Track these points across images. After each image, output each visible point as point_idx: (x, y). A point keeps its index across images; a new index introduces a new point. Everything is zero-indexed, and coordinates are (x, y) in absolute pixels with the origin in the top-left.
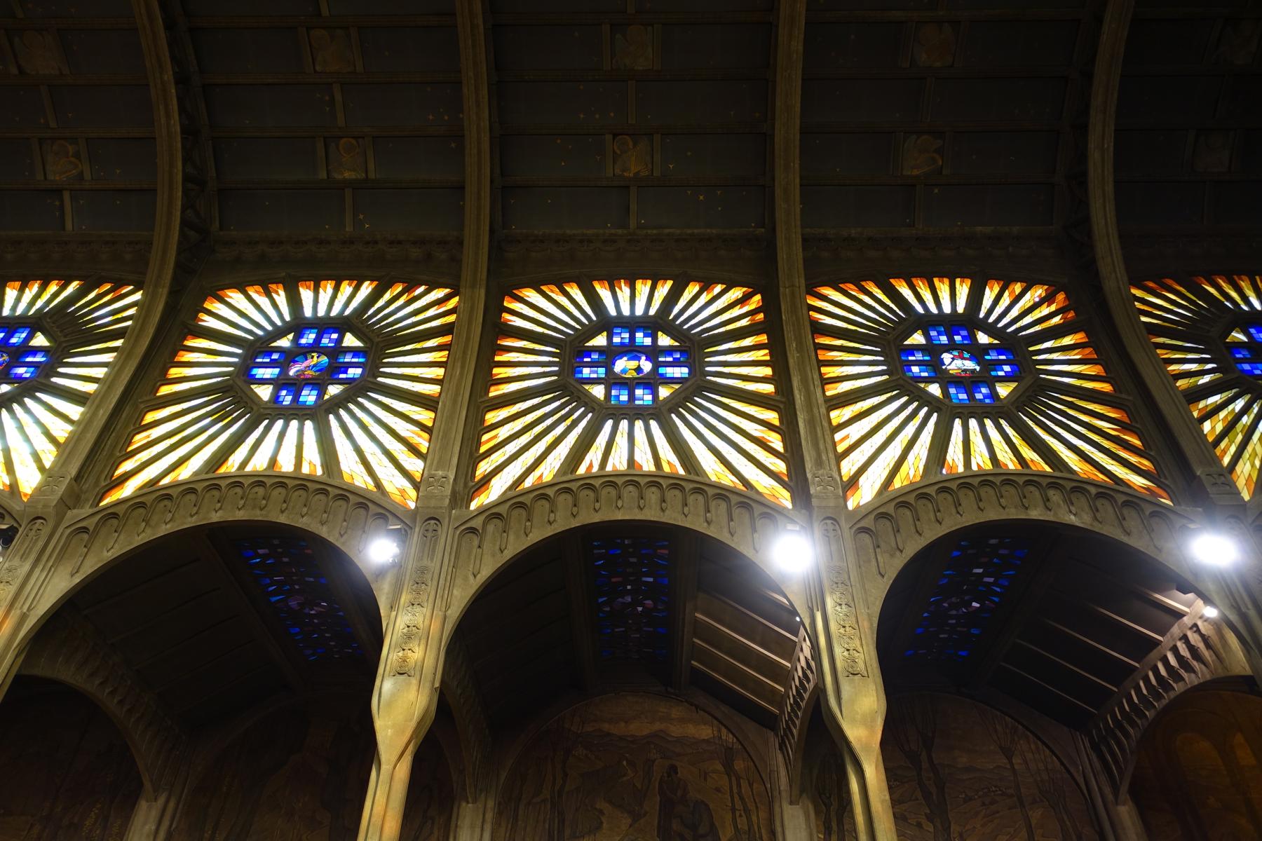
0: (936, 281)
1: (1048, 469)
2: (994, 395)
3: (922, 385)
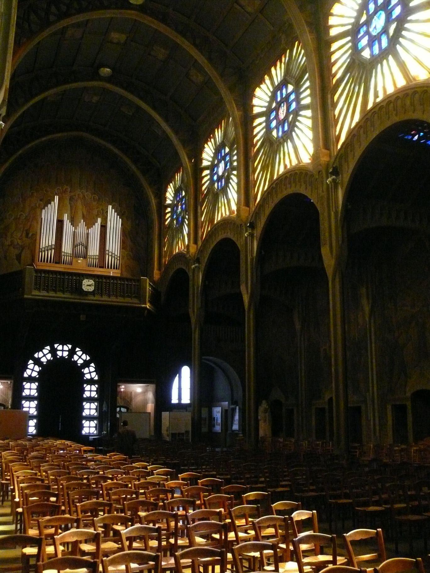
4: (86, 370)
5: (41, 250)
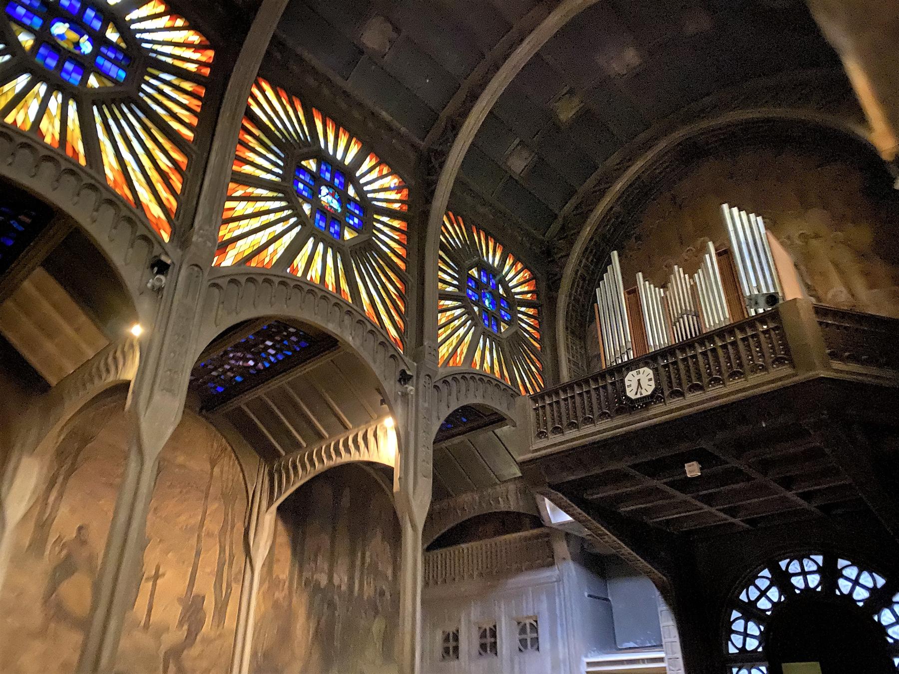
0: (341, 130)
1: (350, 301)
2: (340, 234)
3: (301, 200)
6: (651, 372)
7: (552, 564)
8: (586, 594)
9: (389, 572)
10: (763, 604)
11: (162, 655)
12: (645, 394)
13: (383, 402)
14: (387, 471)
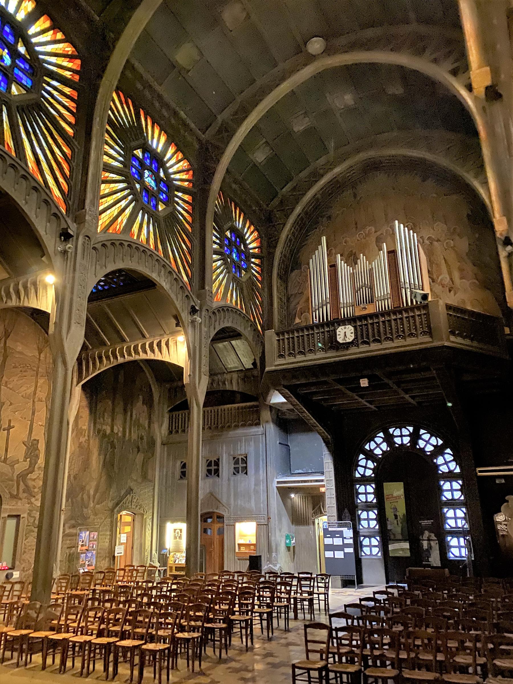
2: (156, 207)
4: (440, 460)
5: (314, 310)
6: (353, 328)
7: (258, 424)
8: (278, 442)
9: (146, 425)
10: (378, 452)
11: (15, 478)
12: (348, 341)
13: (177, 325)
14: (179, 370)
